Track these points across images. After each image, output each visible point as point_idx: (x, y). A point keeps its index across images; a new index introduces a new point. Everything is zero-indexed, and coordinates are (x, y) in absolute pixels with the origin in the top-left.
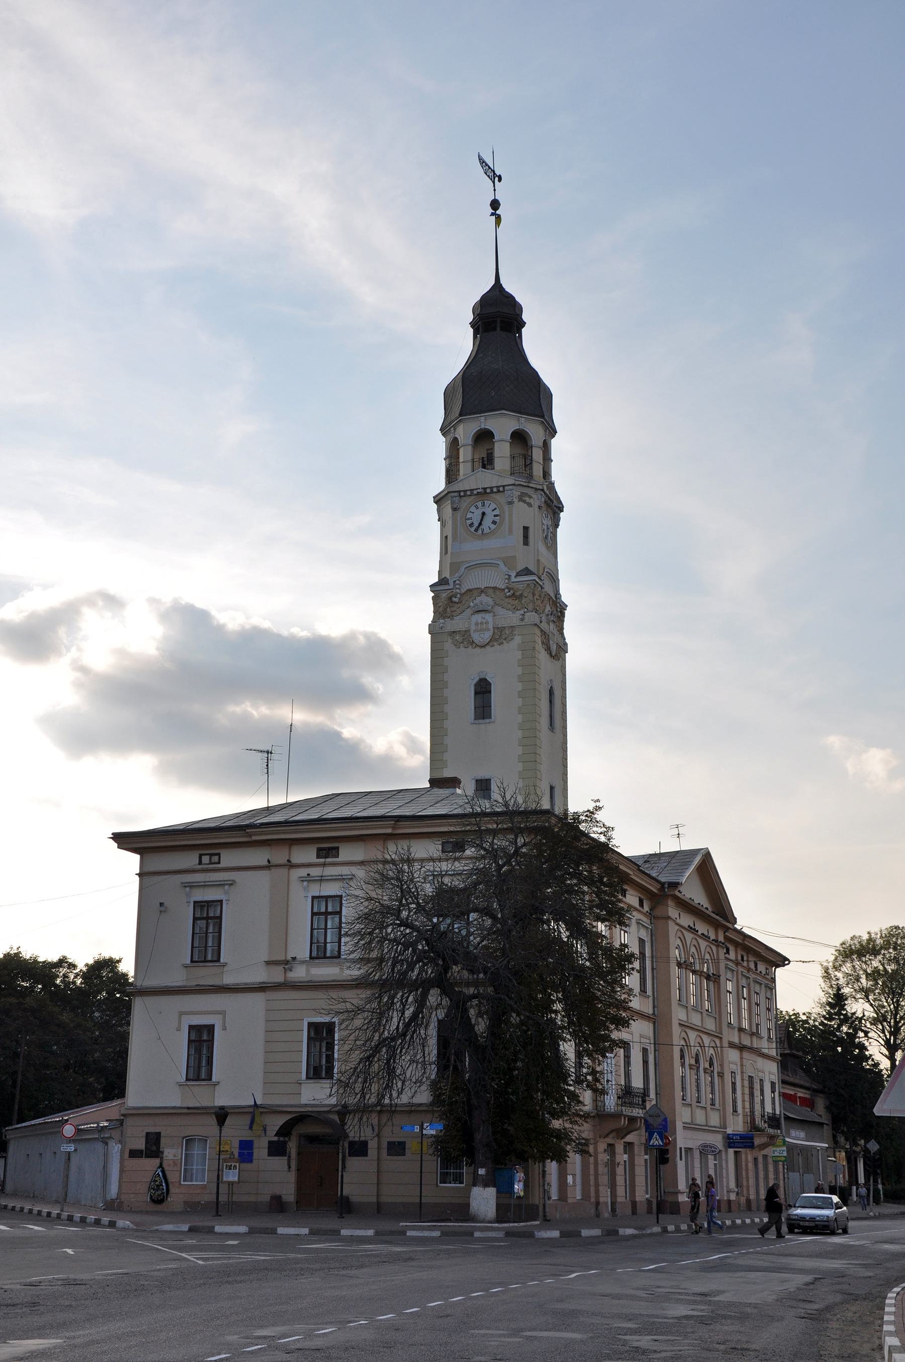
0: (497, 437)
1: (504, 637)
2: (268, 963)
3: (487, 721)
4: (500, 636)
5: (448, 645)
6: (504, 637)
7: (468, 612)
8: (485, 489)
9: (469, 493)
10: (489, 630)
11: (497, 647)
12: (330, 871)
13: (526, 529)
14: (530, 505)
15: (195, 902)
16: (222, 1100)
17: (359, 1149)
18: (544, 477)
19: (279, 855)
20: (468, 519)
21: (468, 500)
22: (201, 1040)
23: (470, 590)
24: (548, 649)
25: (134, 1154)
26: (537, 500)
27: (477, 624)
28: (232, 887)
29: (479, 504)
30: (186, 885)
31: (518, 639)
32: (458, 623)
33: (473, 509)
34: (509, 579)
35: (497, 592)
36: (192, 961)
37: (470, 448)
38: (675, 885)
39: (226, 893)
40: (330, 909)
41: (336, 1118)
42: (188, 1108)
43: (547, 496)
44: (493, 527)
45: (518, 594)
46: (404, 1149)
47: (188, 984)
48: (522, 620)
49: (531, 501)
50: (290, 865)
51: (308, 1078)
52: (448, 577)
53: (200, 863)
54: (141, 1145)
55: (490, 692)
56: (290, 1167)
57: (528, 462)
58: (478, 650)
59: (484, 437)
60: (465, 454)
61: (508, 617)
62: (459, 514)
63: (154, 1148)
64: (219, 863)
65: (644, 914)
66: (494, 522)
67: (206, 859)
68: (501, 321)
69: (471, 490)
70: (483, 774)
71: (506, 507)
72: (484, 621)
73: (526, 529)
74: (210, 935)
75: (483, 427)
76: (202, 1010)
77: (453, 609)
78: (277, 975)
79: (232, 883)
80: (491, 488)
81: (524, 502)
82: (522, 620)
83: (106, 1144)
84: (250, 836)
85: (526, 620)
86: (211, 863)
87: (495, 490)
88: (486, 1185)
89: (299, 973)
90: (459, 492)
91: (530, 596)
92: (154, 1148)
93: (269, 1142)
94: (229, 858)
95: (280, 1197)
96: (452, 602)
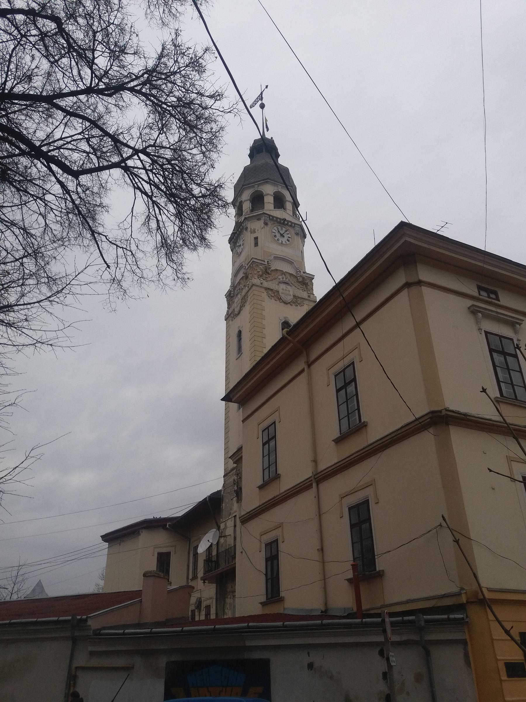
5: (264, 295)
11: (294, 306)
23: (277, 270)
35: (292, 278)
44: (288, 242)
58: (282, 304)
60: (269, 200)
62: (268, 228)
69: (277, 218)
75: (279, 190)
77: (267, 276)
80: (288, 221)
90: (270, 216)
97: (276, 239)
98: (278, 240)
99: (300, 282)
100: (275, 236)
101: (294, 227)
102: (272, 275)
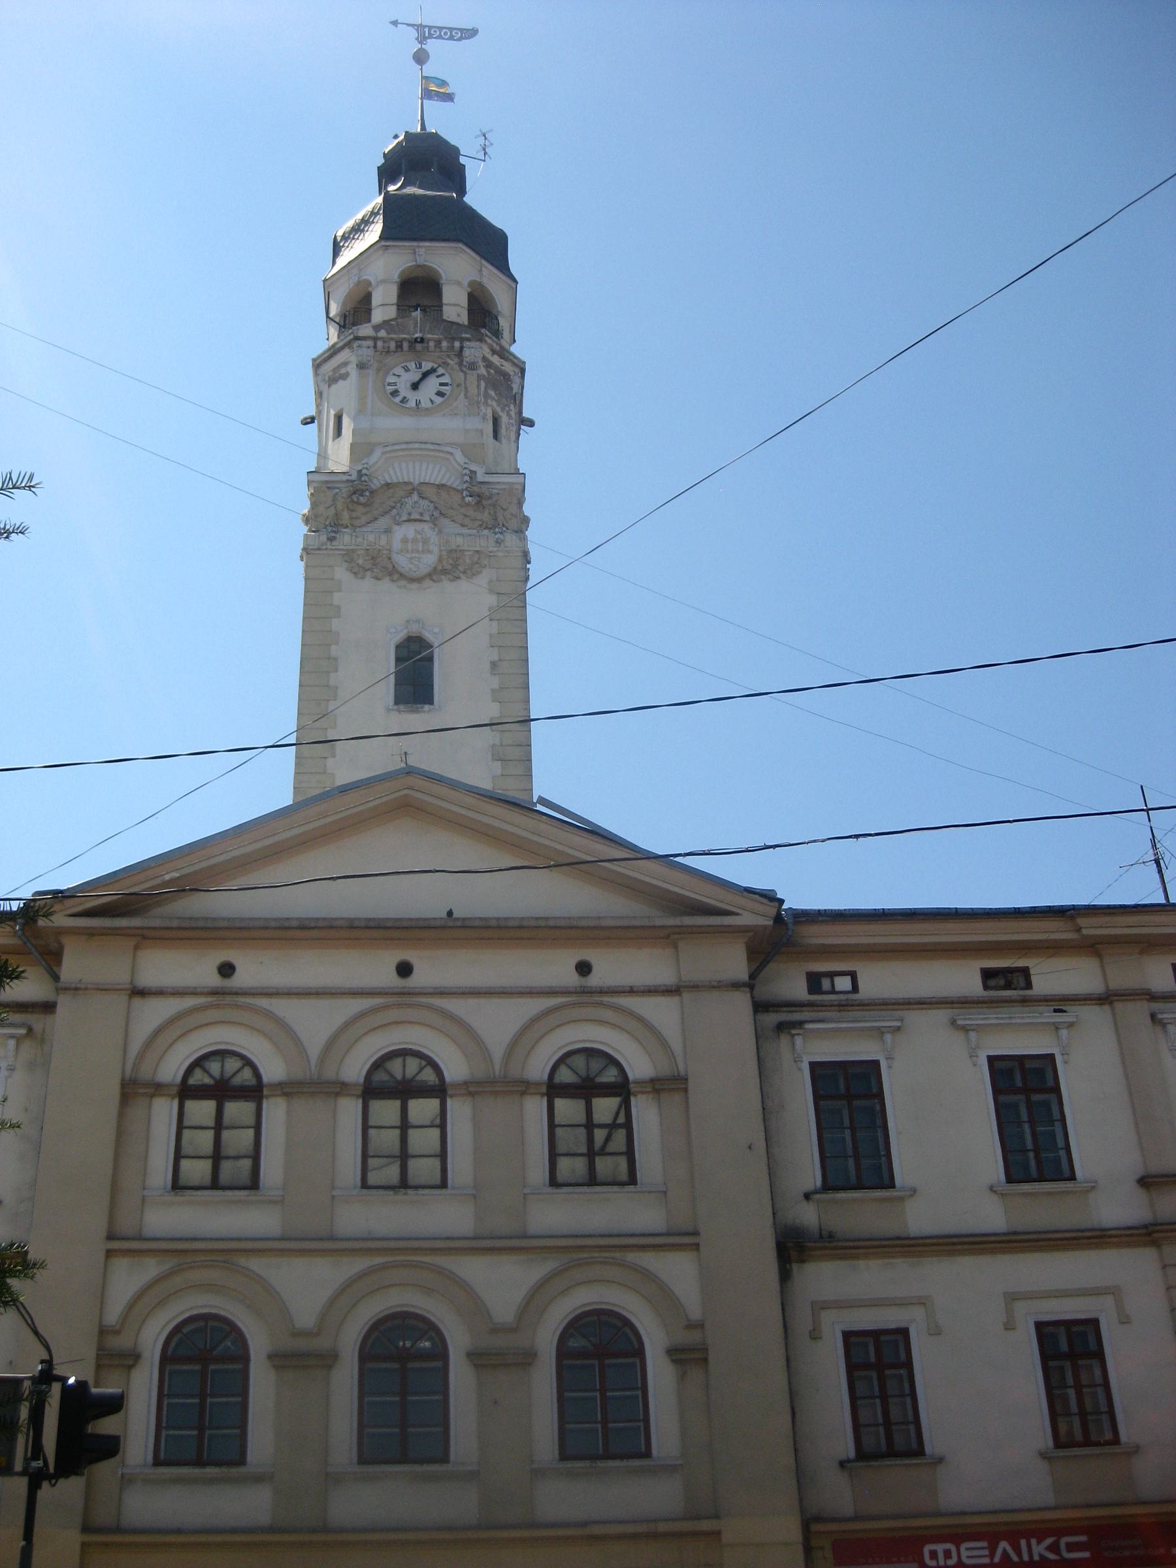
5: (341, 573)
11: (447, 585)
20: (389, 384)
27: (405, 541)
33: (399, 370)
44: (438, 400)
66: (440, 394)
75: (420, 261)
77: (354, 514)
97: (398, 400)
98: (404, 400)
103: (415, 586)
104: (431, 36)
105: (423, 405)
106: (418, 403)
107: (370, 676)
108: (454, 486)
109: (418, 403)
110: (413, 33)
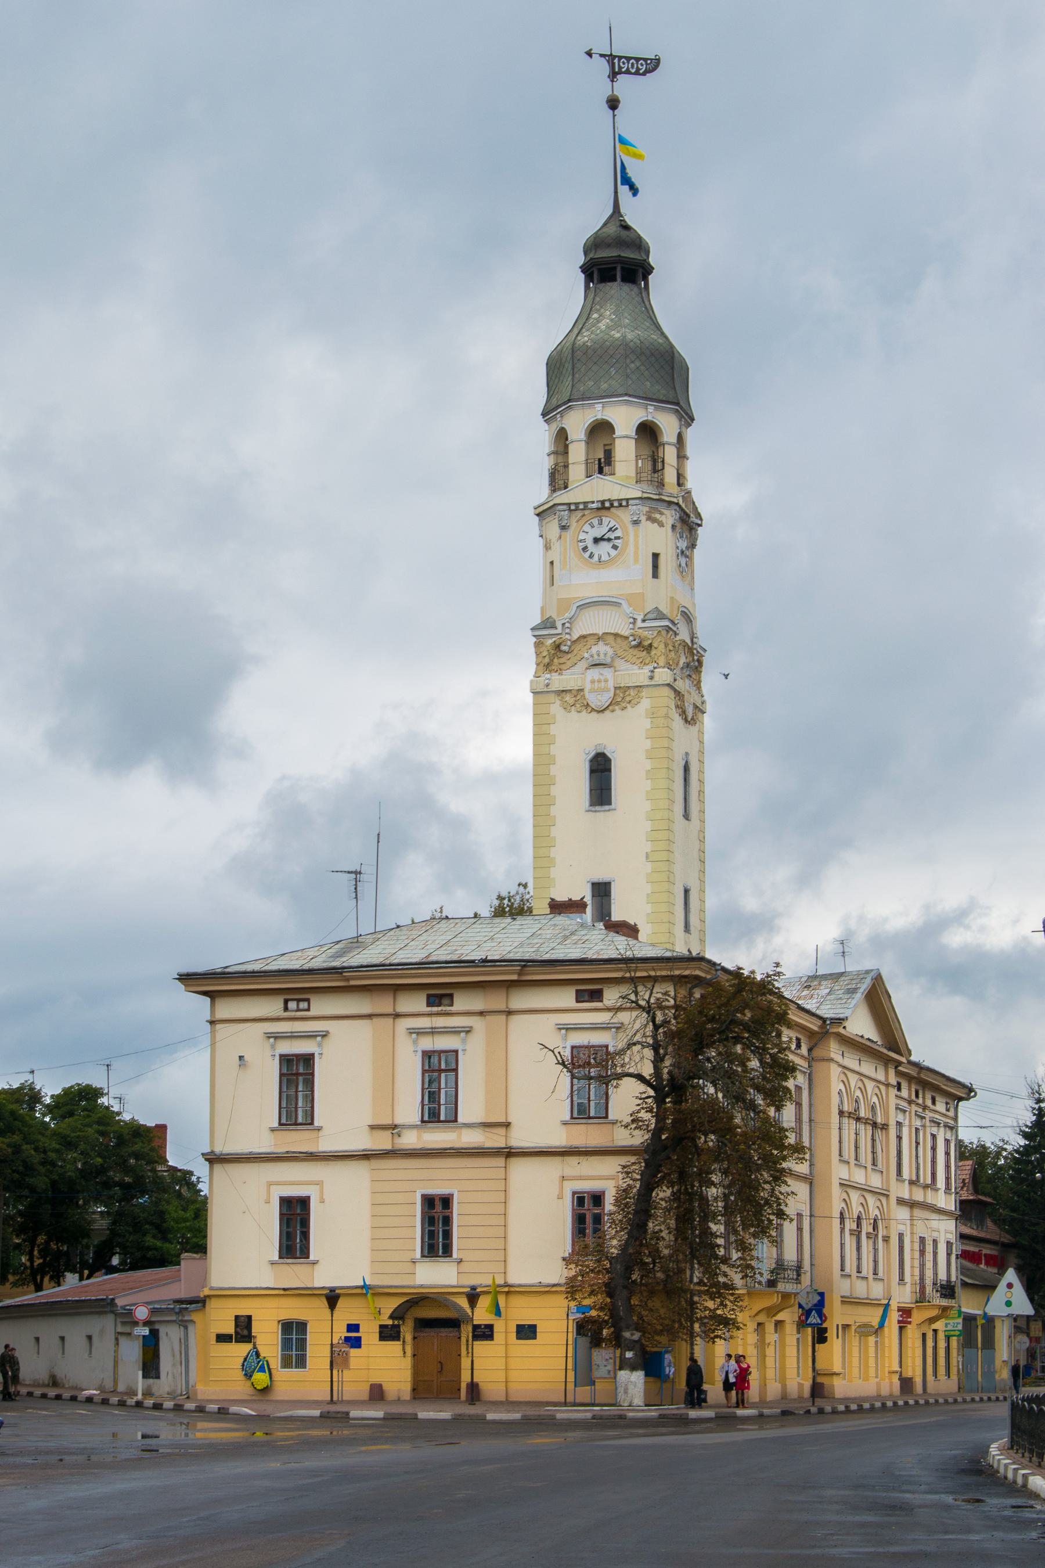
0: (618, 432)
1: (628, 699)
2: (373, 1127)
3: (607, 807)
4: (622, 697)
5: (556, 708)
6: (628, 699)
7: (582, 665)
8: (603, 502)
9: (581, 507)
10: (608, 691)
11: (618, 712)
12: (441, 1022)
13: (656, 556)
14: (661, 524)
15: (281, 1056)
16: (324, 1277)
17: (485, 1333)
18: (679, 485)
19: (384, 1004)
20: (581, 541)
21: (579, 514)
22: (295, 1215)
23: (584, 637)
24: (683, 713)
25: (222, 1338)
26: (669, 517)
27: (593, 682)
28: (326, 1039)
29: (595, 521)
30: (269, 1036)
31: (645, 704)
32: (567, 679)
33: (587, 528)
34: (634, 623)
35: (619, 640)
36: (280, 1124)
37: (583, 444)
38: (839, 1021)
39: (320, 1045)
40: (443, 1066)
41: (464, 1303)
42: (284, 1289)
43: (682, 510)
45: (646, 643)
46: (535, 1332)
47: (276, 1151)
48: (651, 678)
49: (662, 518)
50: (397, 1016)
51: (423, 1256)
52: (554, 617)
53: (286, 1009)
54: (230, 1329)
55: (610, 770)
56: (405, 1353)
57: (656, 465)
58: (594, 714)
59: (601, 430)
60: (578, 452)
61: (634, 673)
62: (568, 535)
63: (245, 1332)
64: (308, 1010)
65: (802, 1057)
67: (292, 1005)
68: (623, 269)
70: (601, 876)
71: (630, 527)
72: (602, 678)
73: (656, 556)
74: (300, 1094)
75: (599, 417)
76: (294, 1180)
78: (383, 1142)
79: (325, 1035)
81: (654, 521)
82: (651, 678)
83: (186, 1328)
84: (348, 979)
85: (656, 678)
86: (298, 1010)
87: (616, 504)
88: (633, 1368)
89: (410, 1140)
90: (569, 504)
91: (662, 647)
92: (245, 1332)
93: (381, 1326)
94: (320, 1006)
95: (380, 1386)
96: (561, 651)
98: (591, 556)
99: (636, 647)
100: (585, 549)
101: (627, 505)
102: (575, 652)
103: (601, 714)
104: (620, 72)
105: (603, 559)
106: (600, 558)
107: (576, 782)
108: (623, 633)
109: (600, 558)
110: (604, 67)
